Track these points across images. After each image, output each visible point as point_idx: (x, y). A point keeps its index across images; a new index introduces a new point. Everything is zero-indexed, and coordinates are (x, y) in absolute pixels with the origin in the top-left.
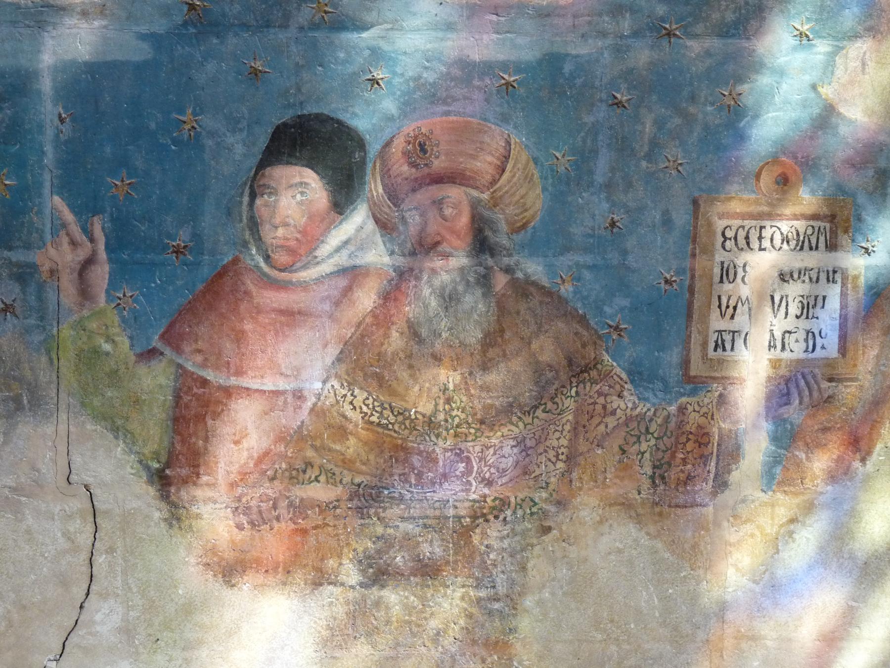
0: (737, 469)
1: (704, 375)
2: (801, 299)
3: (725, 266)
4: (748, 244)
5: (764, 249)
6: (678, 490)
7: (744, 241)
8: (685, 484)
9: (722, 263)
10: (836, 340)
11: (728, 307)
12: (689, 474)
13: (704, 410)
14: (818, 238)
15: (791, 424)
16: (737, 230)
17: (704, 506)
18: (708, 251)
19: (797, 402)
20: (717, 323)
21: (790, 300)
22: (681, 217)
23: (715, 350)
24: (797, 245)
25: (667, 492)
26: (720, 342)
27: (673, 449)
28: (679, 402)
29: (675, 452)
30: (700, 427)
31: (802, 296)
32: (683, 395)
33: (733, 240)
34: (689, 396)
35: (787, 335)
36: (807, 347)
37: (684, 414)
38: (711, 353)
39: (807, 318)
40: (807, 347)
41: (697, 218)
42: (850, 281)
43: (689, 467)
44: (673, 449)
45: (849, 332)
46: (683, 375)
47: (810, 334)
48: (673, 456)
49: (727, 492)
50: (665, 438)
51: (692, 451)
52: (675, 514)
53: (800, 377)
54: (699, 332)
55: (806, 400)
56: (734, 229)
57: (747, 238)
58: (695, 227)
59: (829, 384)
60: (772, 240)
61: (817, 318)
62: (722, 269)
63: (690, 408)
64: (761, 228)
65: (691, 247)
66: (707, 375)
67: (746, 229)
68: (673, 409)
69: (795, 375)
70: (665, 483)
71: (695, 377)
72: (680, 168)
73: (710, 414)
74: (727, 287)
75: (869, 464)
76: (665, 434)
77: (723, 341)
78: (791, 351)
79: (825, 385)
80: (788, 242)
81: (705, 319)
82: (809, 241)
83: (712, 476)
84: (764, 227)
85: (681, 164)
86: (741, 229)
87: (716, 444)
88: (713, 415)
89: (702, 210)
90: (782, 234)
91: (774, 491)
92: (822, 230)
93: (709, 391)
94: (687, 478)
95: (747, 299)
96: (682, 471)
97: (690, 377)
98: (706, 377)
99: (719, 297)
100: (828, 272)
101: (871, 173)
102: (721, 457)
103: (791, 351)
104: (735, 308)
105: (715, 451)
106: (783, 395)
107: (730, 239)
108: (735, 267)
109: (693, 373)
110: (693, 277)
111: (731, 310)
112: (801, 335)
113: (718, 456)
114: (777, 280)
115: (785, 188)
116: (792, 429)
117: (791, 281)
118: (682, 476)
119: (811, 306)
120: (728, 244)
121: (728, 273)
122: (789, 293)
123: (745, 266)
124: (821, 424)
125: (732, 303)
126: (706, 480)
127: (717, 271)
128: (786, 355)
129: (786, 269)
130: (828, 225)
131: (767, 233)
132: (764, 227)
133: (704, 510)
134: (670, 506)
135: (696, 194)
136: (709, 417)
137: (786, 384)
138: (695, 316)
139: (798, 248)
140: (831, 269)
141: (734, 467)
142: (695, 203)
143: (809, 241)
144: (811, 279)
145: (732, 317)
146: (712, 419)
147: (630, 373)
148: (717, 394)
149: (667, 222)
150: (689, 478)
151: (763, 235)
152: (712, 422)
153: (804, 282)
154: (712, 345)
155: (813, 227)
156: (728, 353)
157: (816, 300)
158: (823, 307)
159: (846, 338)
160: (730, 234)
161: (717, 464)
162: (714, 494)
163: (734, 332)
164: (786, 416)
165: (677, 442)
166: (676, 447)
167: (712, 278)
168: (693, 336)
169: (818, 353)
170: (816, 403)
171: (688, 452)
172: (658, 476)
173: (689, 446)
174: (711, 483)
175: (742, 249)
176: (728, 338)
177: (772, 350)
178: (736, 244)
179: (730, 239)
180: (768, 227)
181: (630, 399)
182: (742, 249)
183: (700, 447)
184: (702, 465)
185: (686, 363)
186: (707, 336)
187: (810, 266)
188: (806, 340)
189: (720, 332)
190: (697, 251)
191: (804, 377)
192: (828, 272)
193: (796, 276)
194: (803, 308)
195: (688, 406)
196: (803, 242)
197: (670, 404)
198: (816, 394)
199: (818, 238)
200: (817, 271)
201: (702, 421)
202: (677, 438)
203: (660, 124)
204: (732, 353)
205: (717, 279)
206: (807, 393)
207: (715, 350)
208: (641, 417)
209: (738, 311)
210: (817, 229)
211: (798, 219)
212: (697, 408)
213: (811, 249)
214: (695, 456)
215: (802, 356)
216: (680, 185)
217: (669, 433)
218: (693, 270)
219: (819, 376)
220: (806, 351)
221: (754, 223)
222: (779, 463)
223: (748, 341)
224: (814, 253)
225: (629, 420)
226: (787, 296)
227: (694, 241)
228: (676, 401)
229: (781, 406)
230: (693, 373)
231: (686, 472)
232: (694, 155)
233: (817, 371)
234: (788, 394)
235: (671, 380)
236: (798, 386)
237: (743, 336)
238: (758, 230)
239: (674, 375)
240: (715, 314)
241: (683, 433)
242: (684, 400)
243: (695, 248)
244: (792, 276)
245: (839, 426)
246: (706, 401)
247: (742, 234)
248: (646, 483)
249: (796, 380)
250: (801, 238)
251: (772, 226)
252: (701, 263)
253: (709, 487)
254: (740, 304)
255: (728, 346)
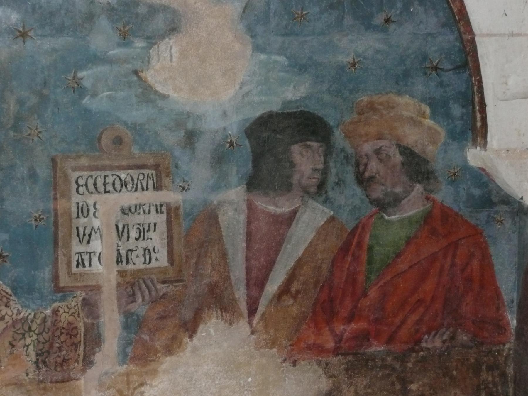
0: (100, 351)
1: (71, 285)
2: (138, 226)
3: (80, 205)
4: (96, 188)
5: (109, 192)
6: (56, 370)
7: (93, 187)
8: (62, 365)
9: (78, 204)
10: (166, 254)
11: (84, 235)
12: (64, 358)
13: (72, 311)
14: (148, 182)
15: (137, 316)
16: (87, 179)
17: (77, 380)
18: (66, 195)
19: (140, 300)
20: (76, 247)
21: (130, 227)
22: (43, 172)
23: (77, 267)
24: (132, 188)
25: (48, 372)
26: (80, 261)
27: (51, 341)
28: (53, 306)
29: (52, 343)
30: (70, 323)
31: (139, 224)
32: (55, 301)
33: (84, 187)
34: (60, 302)
35: (130, 253)
36: (145, 260)
37: (57, 315)
38: (74, 269)
39: (144, 239)
40: (145, 260)
41: (56, 172)
42: (173, 211)
43: (64, 352)
44: (51, 341)
45: (175, 247)
46: (54, 287)
47: (147, 251)
48: (51, 346)
49: (93, 368)
50: (44, 334)
51: (65, 341)
52: (56, 388)
53: (141, 282)
54: (64, 255)
55: (147, 298)
56: (84, 178)
57: (95, 184)
58: (55, 178)
59: (163, 285)
60: (114, 184)
61: (151, 239)
62: (78, 208)
63: (62, 311)
64: (105, 177)
65: (52, 193)
66: (73, 285)
67: (94, 178)
68: (48, 312)
69: (138, 281)
70: (46, 366)
71: (63, 288)
72: (40, 135)
73: (77, 313)
74: (83, 220)
75: (195, 340)
76: (44, 330)
77: (83, 260)
78: (134, 264)
79: (159, 286)
80: (126, 186)
81: (68, 245)
82: (141, 184)
83: (81, 357)
84: (107, 176)
85: (40, 132)
86: (90, 179)
87: (83, 335)
88: (79, 314)
89: (59, 165)
90: (121, 180)
91: (128, 365)
92: (150, 175)
93: (75, 297)
94: (63, 361)
95: (99, 228)
96: (59, 356)
97: (59, 288)
98: (72, 287)
99: (77, 228)
100: (156, 205)
101: (182, 133)
102: (87, 344)
103: (134, 264)
104: (90, 236)
105: (82, 339)
106: (130, 296)
107: (82, 186)
108: (87, 206)
109: (62, 285)
110: (56, 215)
111: (87, 237)
112: (140, 252)
113: (85, 343)
114: (120, 213)
115: (121, 147)
116: (138, 319)
117: (130, 214)
118: (59, 360)
119: (146, 231)
120: (81, 189)
121: (82, 211)
122: (129, 222)
123: (95, 204)
124: (159, 314)
125: (87, 232)
126: (77, 361)
127: (74, 209)
128: (131, 267)
129: (126, 205)
130: (154, 172)
131: (110, 180)
132: (107, 176)
133: (77, 383)
134: (51, 382)
135: (54, 153)
136: (76, 316)
137: (132, 288)
138: (60, 244)
139: (134, 190)
140: (158, 204)
141: (97, 350)
142: (53, 160)
143: (141, 184)
144: (144, 212)
145: (88, 242)
146: (79, 316)
147: (14, 289)
148: (81, 299)
149: (33, 176)
150: (65, 361)
151: (107, 181)
152: (79, 319)
153: (139, 214)
154: (74, 264)
155: (143, 174)
156: (87, 268)
157: (149, 226)
158: (155, 231)
159: (172, 252)
160: (81, 182)
161: (85, 349)
162: (83, 371)
163: (90, 253)
164: (133, 311)
165: (54, 336)
166: (53, 339)
167: (70, 215)
168: (60, 258)
169: (154, 264)
170: (154, 300)
171: (62, 343)
172: (42, 359)
173: (63, 338)
174: (81, 363)
175: (92, 193)
176: (86, 257)
177: (120, 264)
178: (87, 189)
179: (82, 186)
180: (110, 176)
181: (15, 306)
182: (92, 193)
183: (71, 338)
184: (73, 351)
185: (56, 278)
186: (70, 257)
187: (143, 202)
188: (144, 255)
189: (80, 253)
190: (58, 196)
191: (144, 282)
192: (156, 205)
193: (133, 210)
194: (140, 233)
195: (60, 309)
196: (137, 185)
197: (46, 309)
198: (153, 293)
199: (148, 182)
200: (148, 205)
201: (71, 319)
202: (53, 333)
203: (21, 102)
204: (91, 268)
205: (74, 215)
206: (147, 292)
207: (77, 267)
208: (25, 320)
209: (93, 237)
210: (146, 175)
211: (132, 169)
212: (67, 310)
213: (143, 189)
214: (68, 344)
215: (142, 267)
216: (41, 148)
217: (46, 330)
218: (56, 210)
219: (155, 280)
220: (145, 263)
221: (99, 173)
222: (130, 344)
223: (101, 259)
224: (145, 192)
225: (14, 323)
226: (128, 225)
227: (55, 189)
228: (51, 306)
229: (129, 304)
230: (62, 285)
231: (62, 357)
232: (50, 125)
233: (153, 277)
234: (134, 294)
235: (45, 291)
236: (140, 289)
237: (97, 255)
238: (103, 178)
239: (47, 287)
240: (75, 241)
241: (58, 329)
242: (56, 305)
243: (56, 194)
244: (130, 210)
245: (171, 314)
246: (73, 304)
247: (91, 182)
248: (32, 367)
249: (139, 284)
250: (135, 182)
251: (113, 175)
252: (62, 204)
253: (80, 366)
254: (93, 232)
255: (87, 263)
